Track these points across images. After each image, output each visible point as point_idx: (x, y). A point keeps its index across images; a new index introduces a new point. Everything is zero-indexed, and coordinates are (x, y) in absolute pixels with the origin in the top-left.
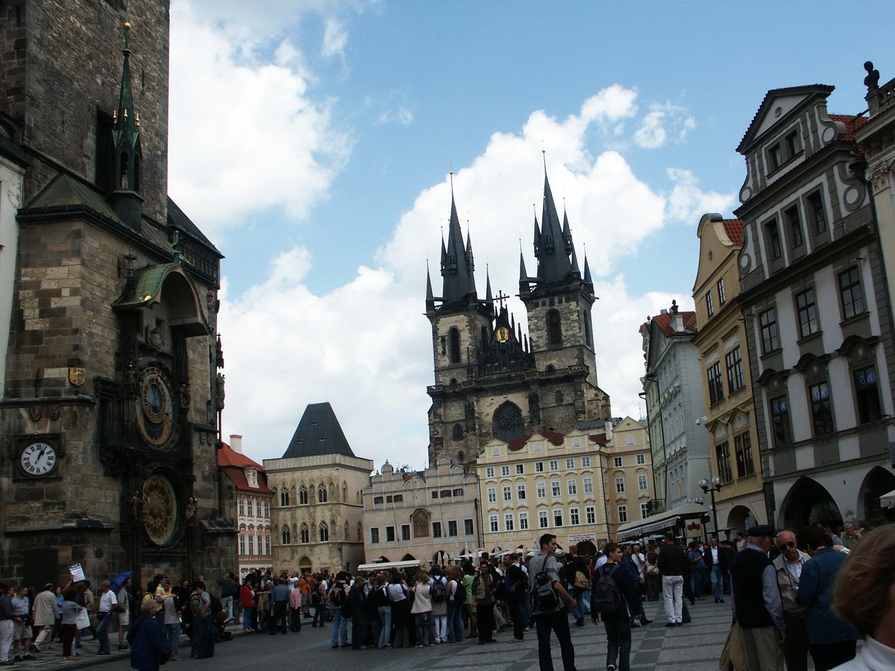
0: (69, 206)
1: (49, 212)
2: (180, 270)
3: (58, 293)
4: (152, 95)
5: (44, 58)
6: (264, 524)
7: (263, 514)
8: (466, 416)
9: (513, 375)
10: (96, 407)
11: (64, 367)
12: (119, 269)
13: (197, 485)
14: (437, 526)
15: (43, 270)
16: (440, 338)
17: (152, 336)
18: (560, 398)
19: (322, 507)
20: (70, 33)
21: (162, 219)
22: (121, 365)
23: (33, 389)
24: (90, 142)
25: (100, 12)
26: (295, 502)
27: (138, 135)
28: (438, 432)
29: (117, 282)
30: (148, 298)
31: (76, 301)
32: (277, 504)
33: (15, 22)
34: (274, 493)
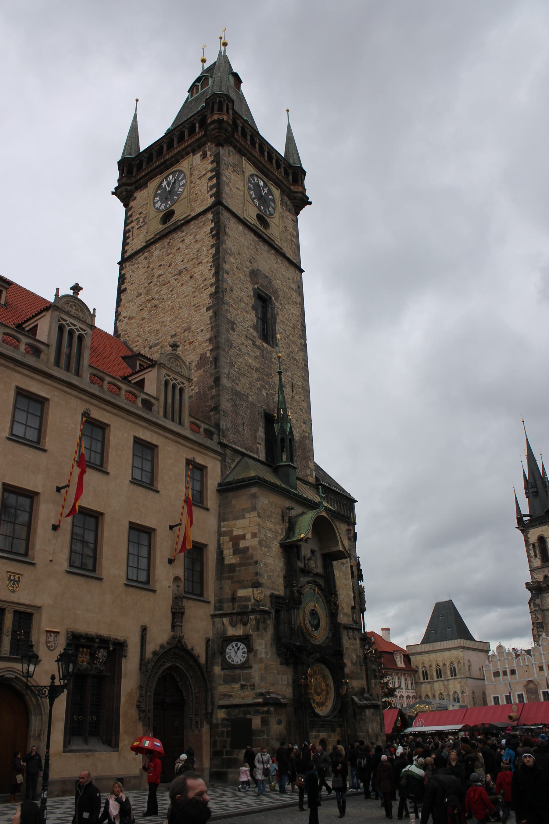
0: (249, 477)
1: (236, 483)
2: (324, 514)
3: (243, 537)
4: (299, 397)
6: (411, 695)
10: (273, 615)
12: (283, 517)
13: (347, 670)
15: (234, 522)
16: (531, 545)
17: (308, 562)
19: (453, 680)
21: (312, 480)
23: (231, 604)
24: (261, 433)
25: (263, 351)
26: (432, 677)
27: (291, 425)
28: (538, 618)
29: (282, 526)
30: (302, 536)
31: (255, 542)
32: (420, 679)
33: (213, 367)
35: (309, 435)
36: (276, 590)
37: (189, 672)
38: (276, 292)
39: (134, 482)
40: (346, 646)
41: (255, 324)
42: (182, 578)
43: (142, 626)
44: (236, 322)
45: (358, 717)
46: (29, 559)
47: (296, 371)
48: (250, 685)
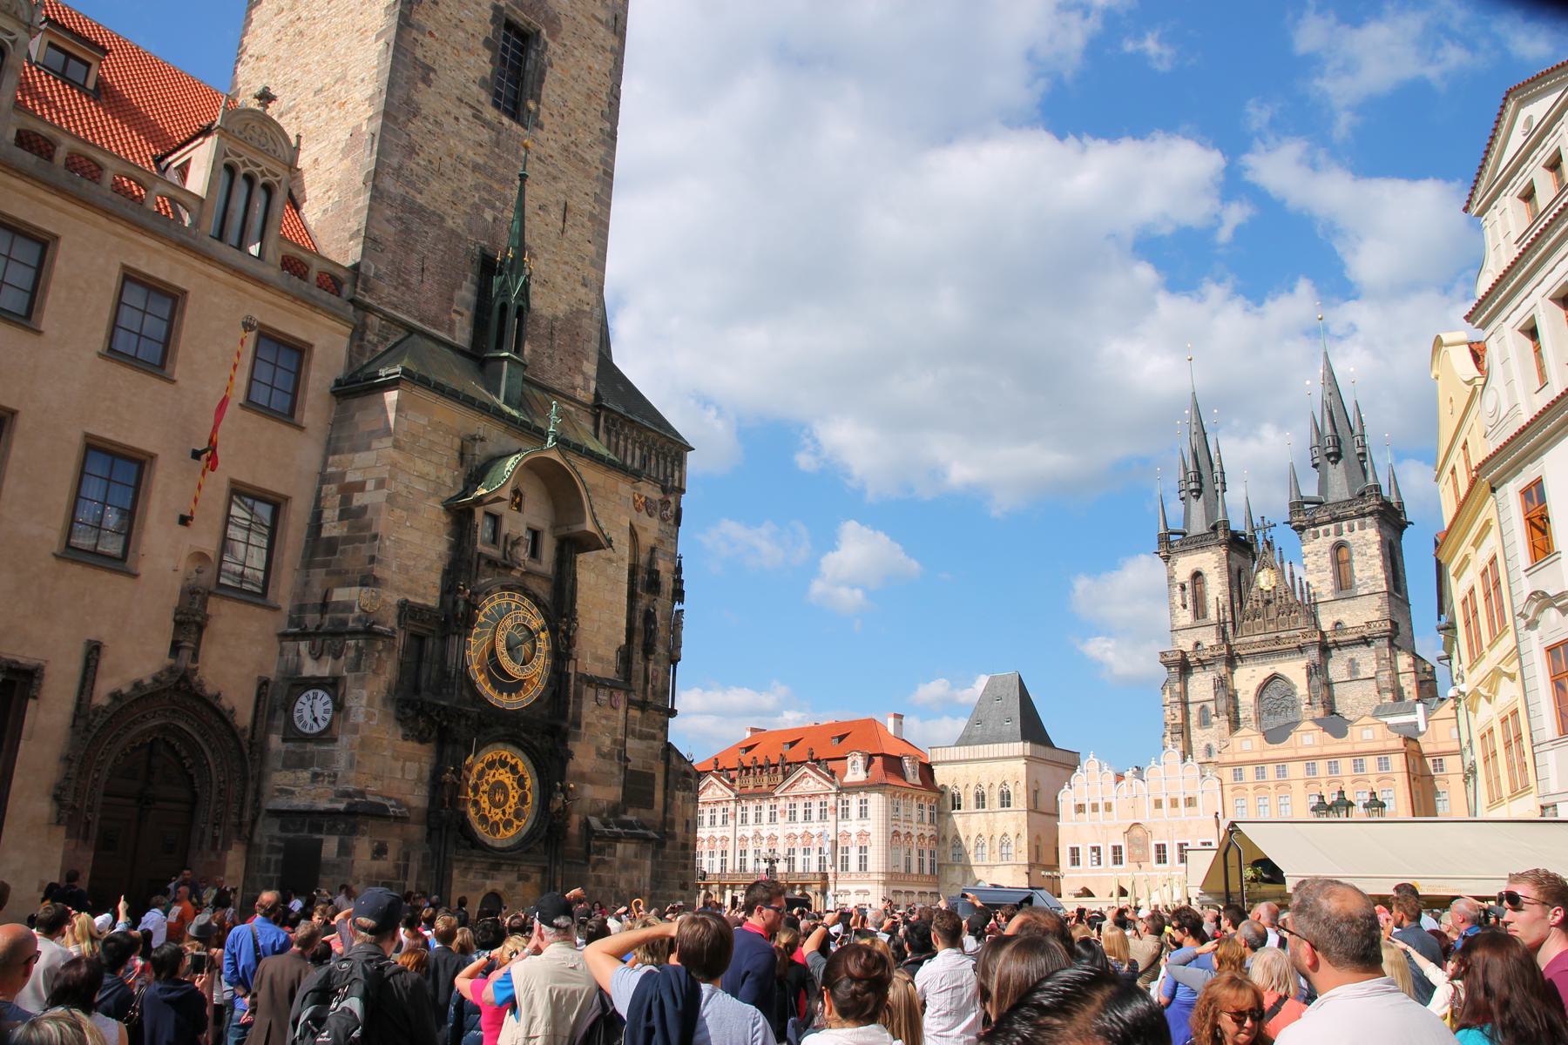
1: (366, 380)
3: (360, 487)
5: (401, 191)
7: (927, 818)
8: (1216, 694)
9: (1283, 635)
11: (355, 586)
12: (462, 455)
13: (572, 766)
14: (1161, 849)
15: (350, 456)
17: (512, 548)
18: (1353, 666)
20: (448, 160)
22: (449, 588)
23: (318, 615)
24: (466, 293)
25: (499, 133)
32: (946, 807)
33: (368, 152)
34: (943, 793)
35: (592, 309)
36: (416, 595)
37: (207, 740)
38: (553, 22)
39: (112, 352)
40: (589, 720)
41: (488, 77)
42: (212, 556)
43: (89, 641)
44: (436, 67)
45: (594, 857)
47: (581, 182)
48: (329, 776)
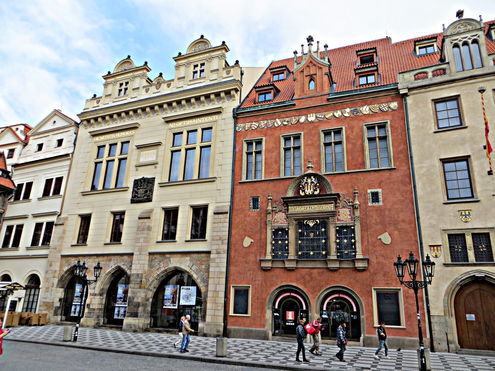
46: (475, 199)
